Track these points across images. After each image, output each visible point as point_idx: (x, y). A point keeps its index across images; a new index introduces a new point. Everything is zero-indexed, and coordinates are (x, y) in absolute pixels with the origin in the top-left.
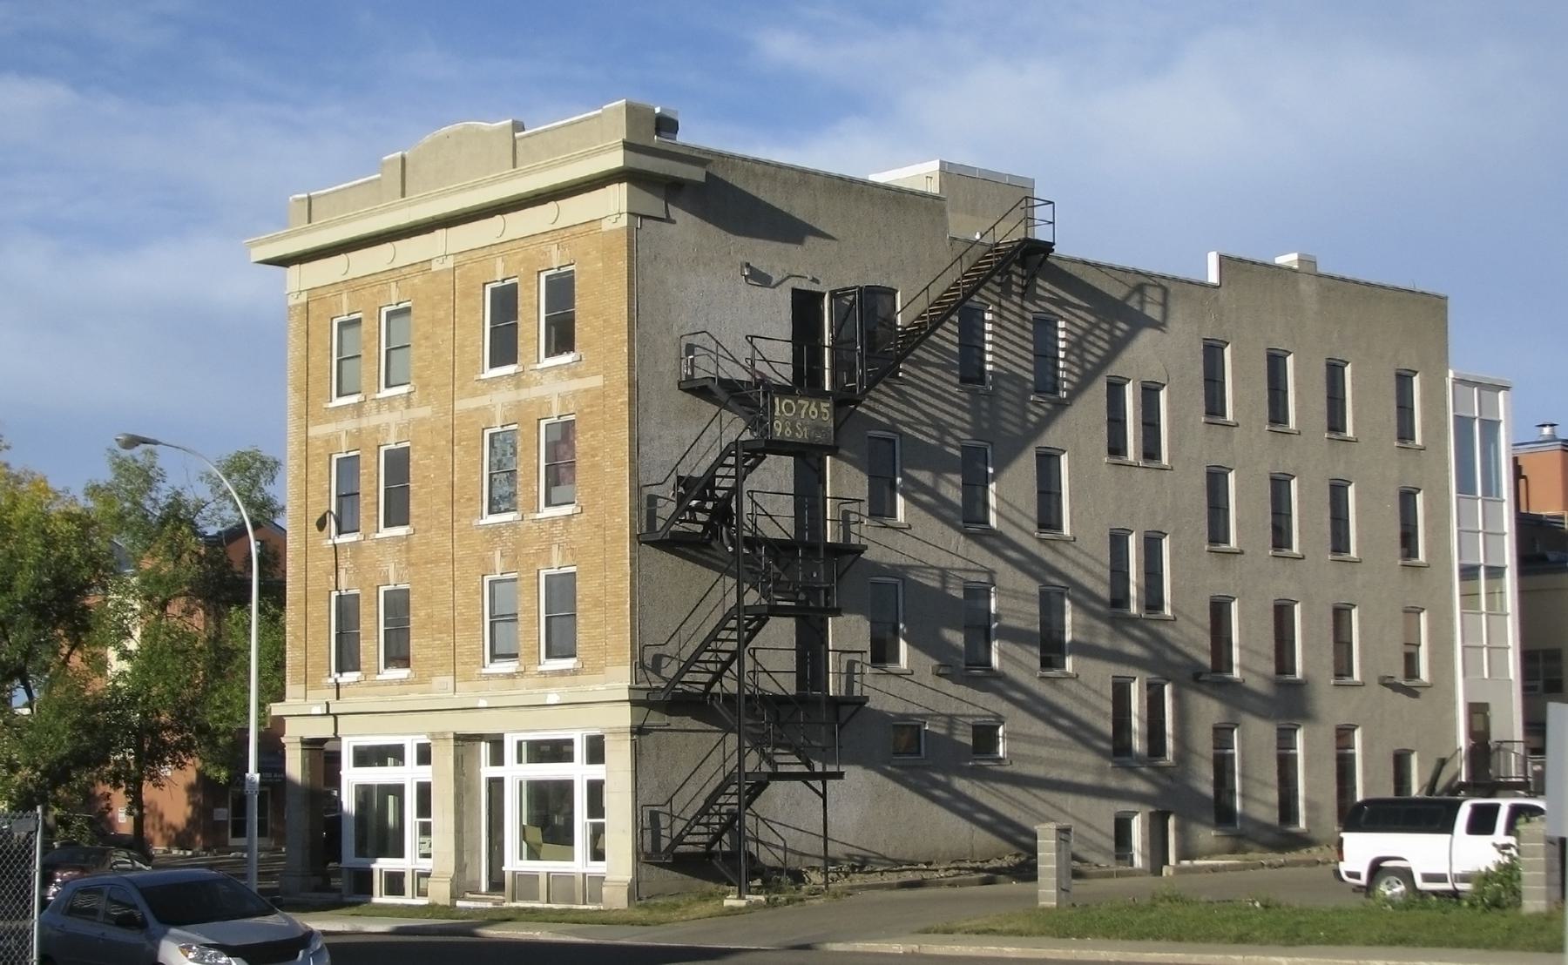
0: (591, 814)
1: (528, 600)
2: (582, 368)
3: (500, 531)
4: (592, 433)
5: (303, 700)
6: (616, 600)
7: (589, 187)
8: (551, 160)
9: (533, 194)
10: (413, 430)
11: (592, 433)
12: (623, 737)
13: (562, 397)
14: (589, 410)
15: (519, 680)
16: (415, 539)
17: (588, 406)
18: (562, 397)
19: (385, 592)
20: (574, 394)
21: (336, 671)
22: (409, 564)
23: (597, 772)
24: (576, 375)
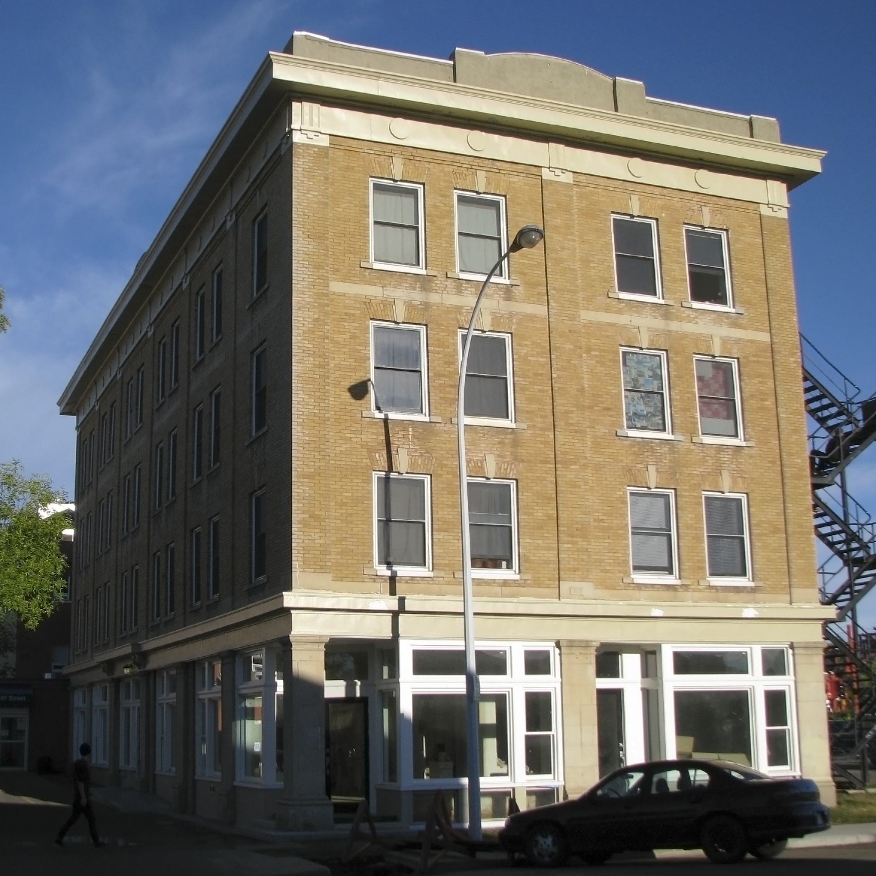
0: (771, 721)
1: (691, 518)
2: (743, 321)
3: (652, 448)
4: (761, 380)
5: (558, 600)
6: (800, 530)
7: (622, 151)
8: (767, 142)
9: (698, 156)
10: (517, 324)
11: (761, 380)
12: (316, 646)
13: (725, 341)
14: (755, 359)
15: (681, 594)
16: (746, 451)
17: (754, 356)
18: (725, 341)
19: (740, 500)
20: (737, 341)
21: (380, 563)
22: (516, 459)
23: (776, 683)
24: (735, 325)
